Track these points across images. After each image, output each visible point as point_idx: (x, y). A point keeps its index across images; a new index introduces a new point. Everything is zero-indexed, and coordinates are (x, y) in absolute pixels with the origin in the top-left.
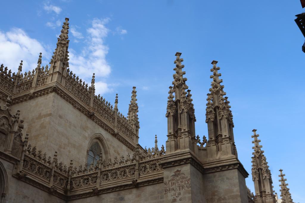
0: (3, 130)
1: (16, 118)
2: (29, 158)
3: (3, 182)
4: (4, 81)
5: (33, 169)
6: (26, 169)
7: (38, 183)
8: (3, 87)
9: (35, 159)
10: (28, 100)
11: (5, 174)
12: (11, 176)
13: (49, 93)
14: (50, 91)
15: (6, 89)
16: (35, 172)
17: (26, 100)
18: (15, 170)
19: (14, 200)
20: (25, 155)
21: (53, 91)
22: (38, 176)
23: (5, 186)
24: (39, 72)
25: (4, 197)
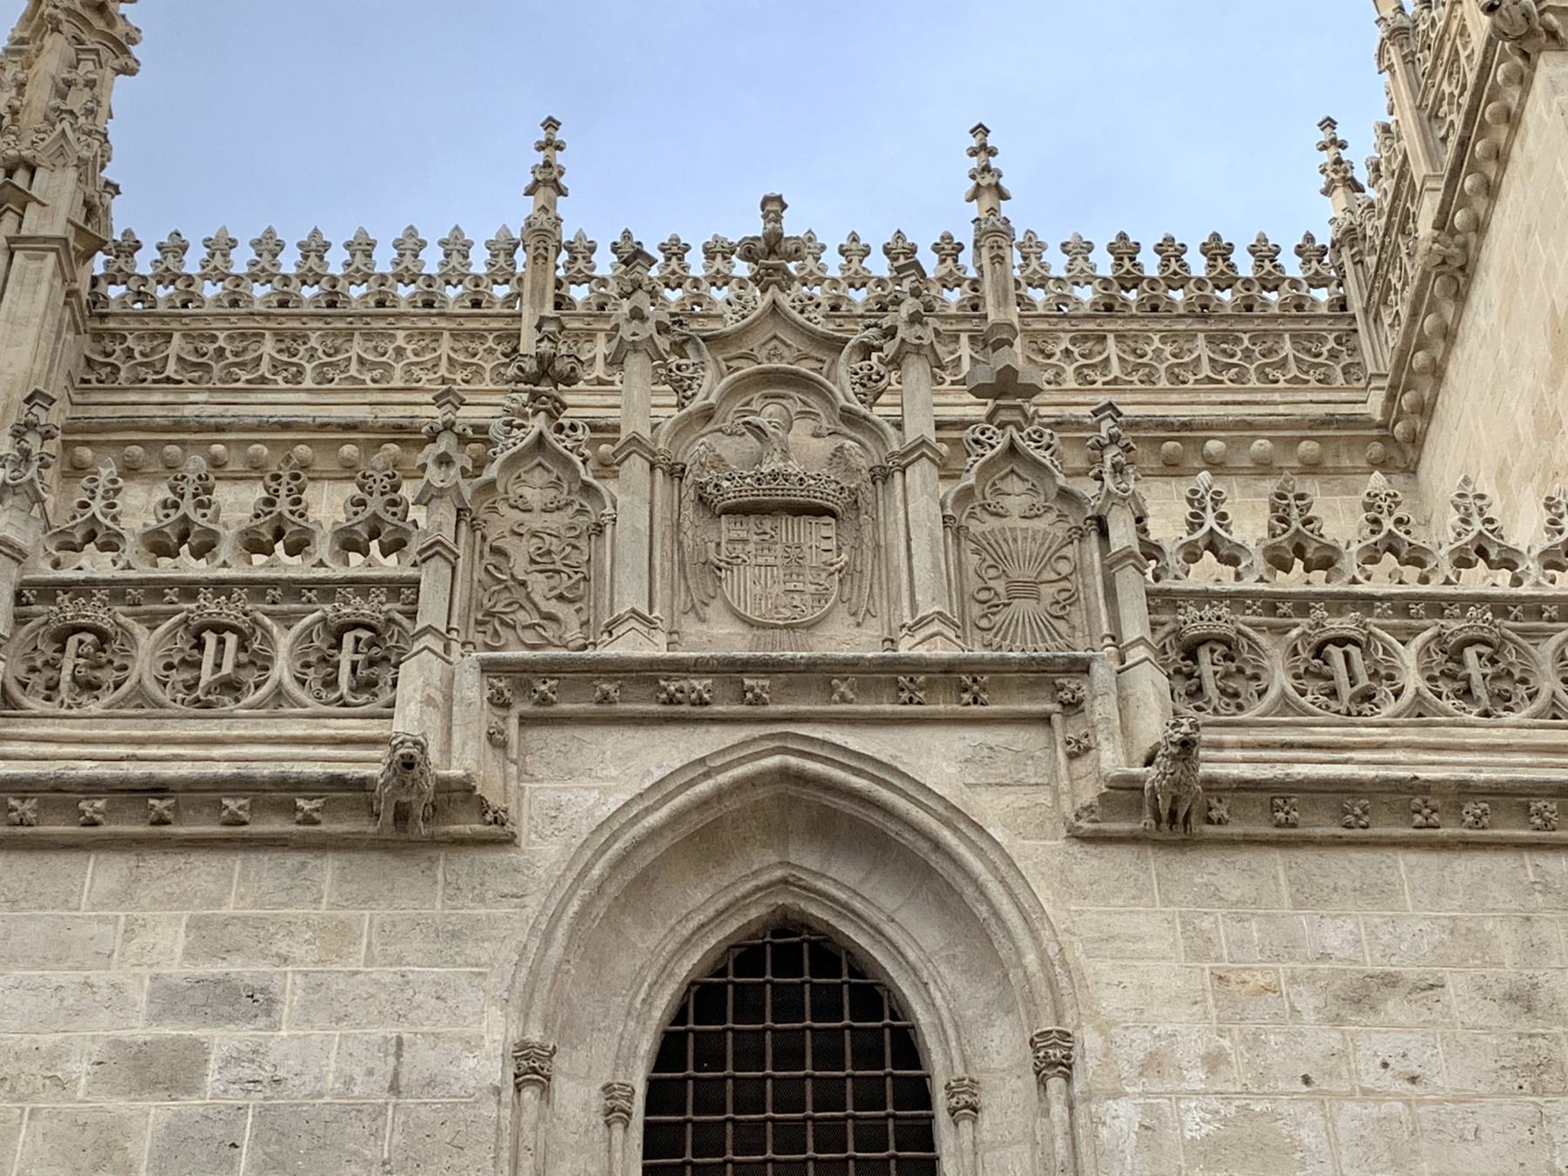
0: (775, 476)
2: (1237, 600)
3: (998, 936)
4: (1238, 341)
5: (1346, 692)
7: (1465, 789)
8: (1254, 383)
9: (1337, 587)
10: (1459, 316)
11: (980, 853)
12: (1061, 843)
13: (1521, 106)
14: (1508, 79)
15: (1295, 380)
16: (1389, 708)
17: (1449, 335)
18: (1080, 766)
19: (1214, 1061)
20: (1162, 601)
21: (1525, 55)
23: (1031, 959)
24: (1409, 60)
25: (1065, 1068)
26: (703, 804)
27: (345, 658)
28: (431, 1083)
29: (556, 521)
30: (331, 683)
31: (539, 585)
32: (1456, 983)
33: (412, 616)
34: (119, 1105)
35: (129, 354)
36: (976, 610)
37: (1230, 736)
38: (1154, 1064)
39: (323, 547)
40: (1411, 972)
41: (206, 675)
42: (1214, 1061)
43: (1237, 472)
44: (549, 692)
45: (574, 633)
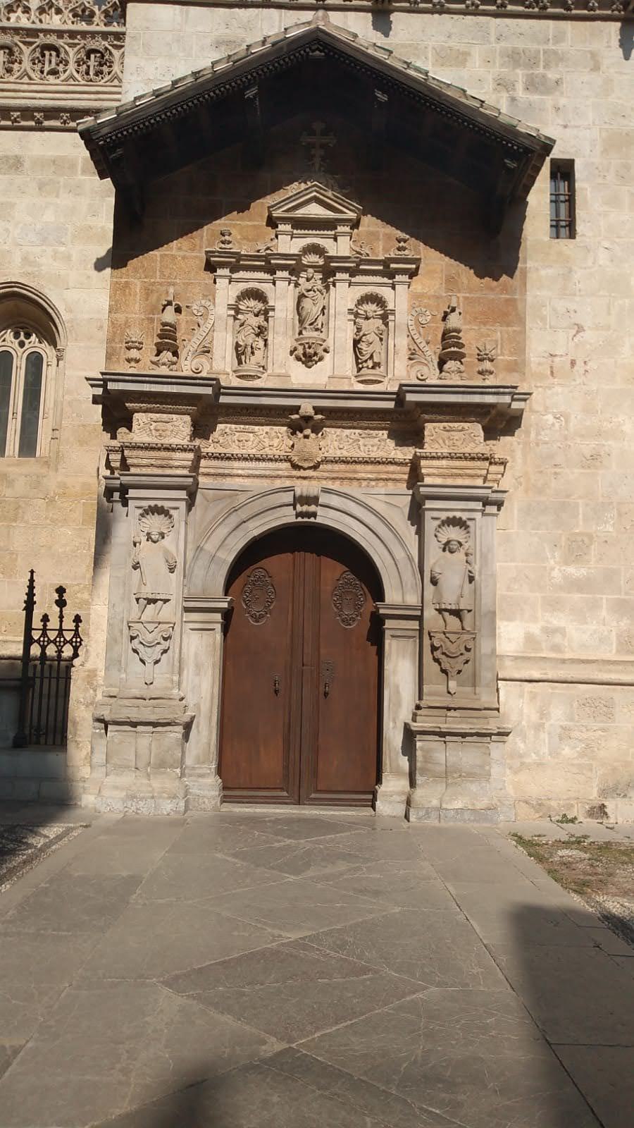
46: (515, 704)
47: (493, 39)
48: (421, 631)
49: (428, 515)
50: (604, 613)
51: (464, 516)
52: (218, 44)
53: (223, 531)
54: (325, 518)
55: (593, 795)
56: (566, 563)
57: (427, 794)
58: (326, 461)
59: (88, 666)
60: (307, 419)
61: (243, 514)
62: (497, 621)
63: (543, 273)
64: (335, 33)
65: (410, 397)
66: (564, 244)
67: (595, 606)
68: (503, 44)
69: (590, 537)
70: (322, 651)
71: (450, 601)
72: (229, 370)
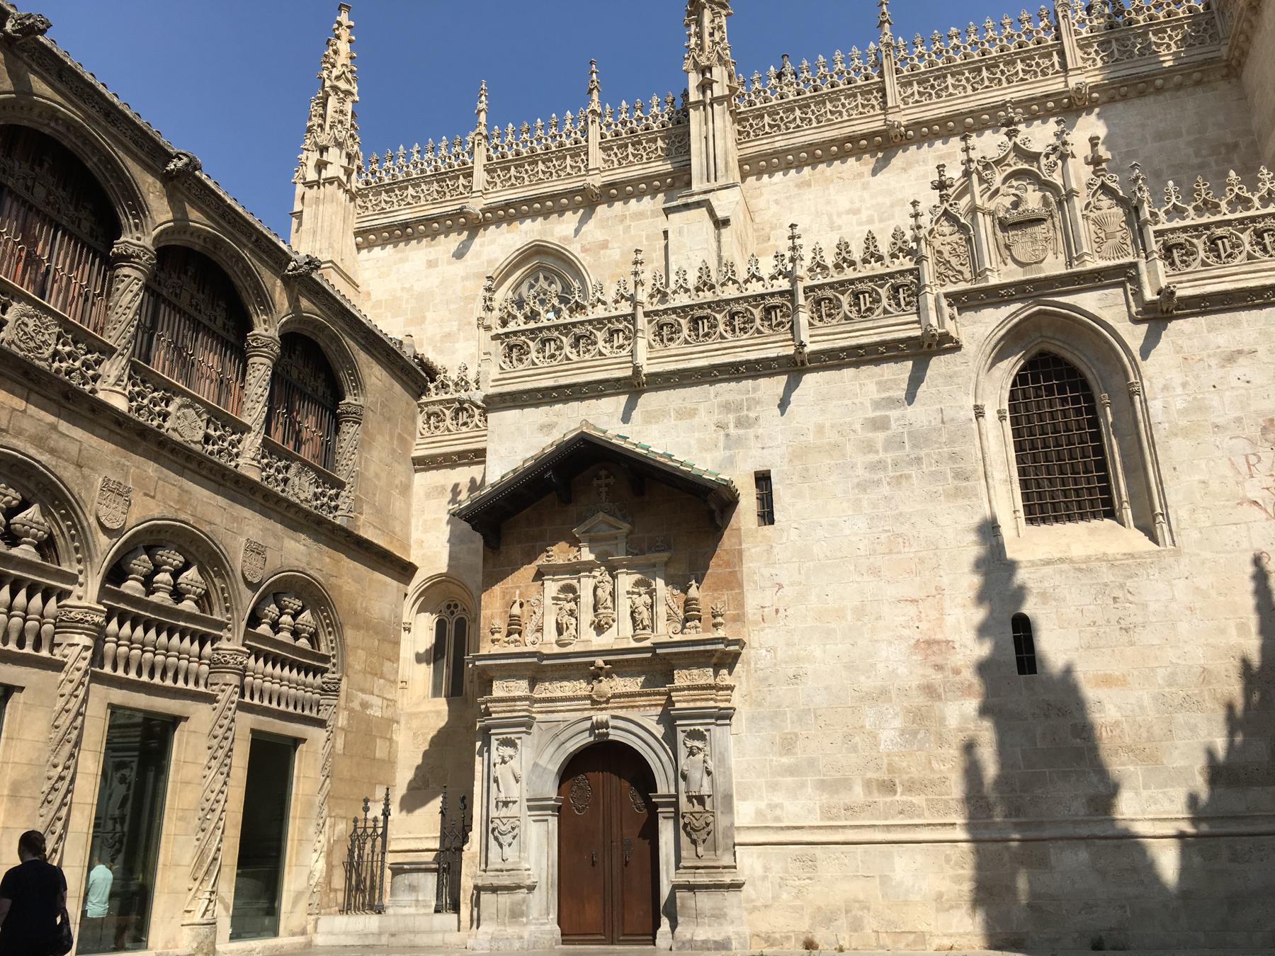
1: (1055, 149)
5: (1223, 255)
6: (1189, 270)
19: (1184, 385)
22: (1263, 266)
26: (1016, 325)
27: (901, 296)
28: (952, 420)
29: (956, 237)
30: (898, 304)
31: (954, 261)
32: (1262, 350)
33: (918, 279)
34: (870, 435)
35: (751, 125)
36: (1095, 246)
37: (1184, 278)
38: (1166, 388)
39: (887, 260)
40: (1246, 348)
41: (863, 308)
42: (1184, 385)
43: (1168, 90)
44: (966, 302)
45: (968, 275)
46: (748, 863)
47: (712, 396)
48: (677, 811)
49: (679, 729)
50: (810, 790)
51: (701, 728)
52: (542, 428)
53: (551, 749)
54: (614, 735)
55: (803, 926)
56: (781, 755)
57: (684, 931)
58: (614, 696)
59: (472, 850)
60: (601, 668)
61: (562, 738)
62: (736, 802)
63: (753, 550)
64: (593, 432)
65: (658, 651)
66: (768, 529)
67: (803, 785)
68: (719, 399)
69: (796, 735)
70: (625, 831)
71: (695, 790)
72: (554, 641)
